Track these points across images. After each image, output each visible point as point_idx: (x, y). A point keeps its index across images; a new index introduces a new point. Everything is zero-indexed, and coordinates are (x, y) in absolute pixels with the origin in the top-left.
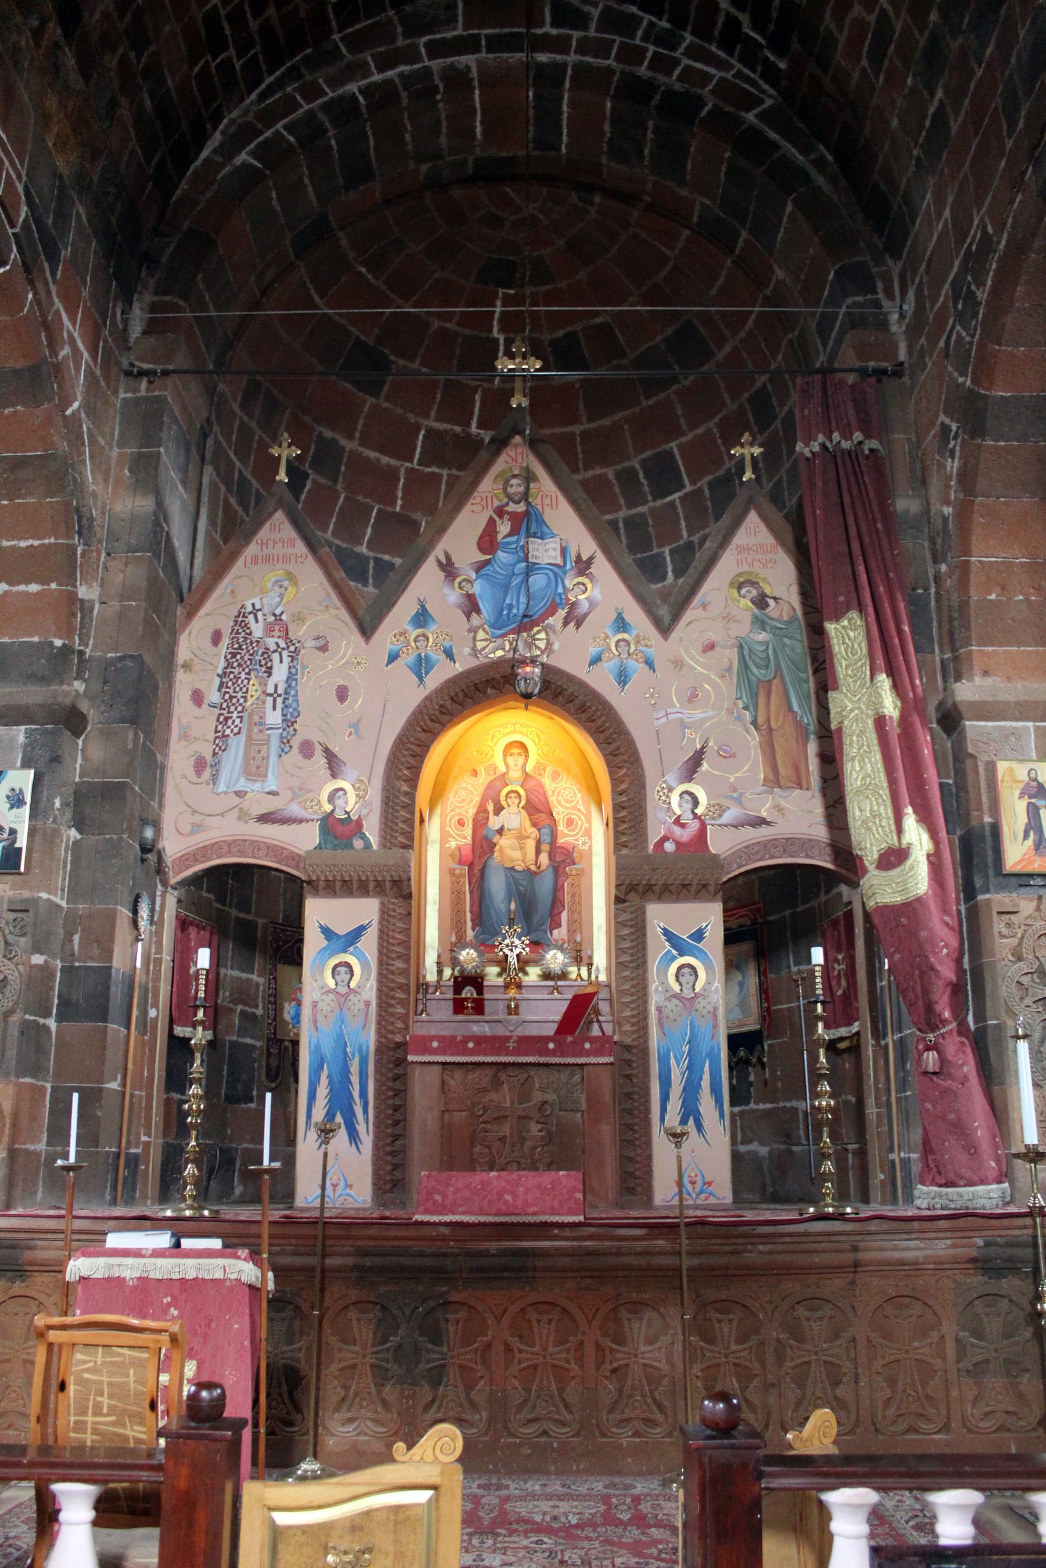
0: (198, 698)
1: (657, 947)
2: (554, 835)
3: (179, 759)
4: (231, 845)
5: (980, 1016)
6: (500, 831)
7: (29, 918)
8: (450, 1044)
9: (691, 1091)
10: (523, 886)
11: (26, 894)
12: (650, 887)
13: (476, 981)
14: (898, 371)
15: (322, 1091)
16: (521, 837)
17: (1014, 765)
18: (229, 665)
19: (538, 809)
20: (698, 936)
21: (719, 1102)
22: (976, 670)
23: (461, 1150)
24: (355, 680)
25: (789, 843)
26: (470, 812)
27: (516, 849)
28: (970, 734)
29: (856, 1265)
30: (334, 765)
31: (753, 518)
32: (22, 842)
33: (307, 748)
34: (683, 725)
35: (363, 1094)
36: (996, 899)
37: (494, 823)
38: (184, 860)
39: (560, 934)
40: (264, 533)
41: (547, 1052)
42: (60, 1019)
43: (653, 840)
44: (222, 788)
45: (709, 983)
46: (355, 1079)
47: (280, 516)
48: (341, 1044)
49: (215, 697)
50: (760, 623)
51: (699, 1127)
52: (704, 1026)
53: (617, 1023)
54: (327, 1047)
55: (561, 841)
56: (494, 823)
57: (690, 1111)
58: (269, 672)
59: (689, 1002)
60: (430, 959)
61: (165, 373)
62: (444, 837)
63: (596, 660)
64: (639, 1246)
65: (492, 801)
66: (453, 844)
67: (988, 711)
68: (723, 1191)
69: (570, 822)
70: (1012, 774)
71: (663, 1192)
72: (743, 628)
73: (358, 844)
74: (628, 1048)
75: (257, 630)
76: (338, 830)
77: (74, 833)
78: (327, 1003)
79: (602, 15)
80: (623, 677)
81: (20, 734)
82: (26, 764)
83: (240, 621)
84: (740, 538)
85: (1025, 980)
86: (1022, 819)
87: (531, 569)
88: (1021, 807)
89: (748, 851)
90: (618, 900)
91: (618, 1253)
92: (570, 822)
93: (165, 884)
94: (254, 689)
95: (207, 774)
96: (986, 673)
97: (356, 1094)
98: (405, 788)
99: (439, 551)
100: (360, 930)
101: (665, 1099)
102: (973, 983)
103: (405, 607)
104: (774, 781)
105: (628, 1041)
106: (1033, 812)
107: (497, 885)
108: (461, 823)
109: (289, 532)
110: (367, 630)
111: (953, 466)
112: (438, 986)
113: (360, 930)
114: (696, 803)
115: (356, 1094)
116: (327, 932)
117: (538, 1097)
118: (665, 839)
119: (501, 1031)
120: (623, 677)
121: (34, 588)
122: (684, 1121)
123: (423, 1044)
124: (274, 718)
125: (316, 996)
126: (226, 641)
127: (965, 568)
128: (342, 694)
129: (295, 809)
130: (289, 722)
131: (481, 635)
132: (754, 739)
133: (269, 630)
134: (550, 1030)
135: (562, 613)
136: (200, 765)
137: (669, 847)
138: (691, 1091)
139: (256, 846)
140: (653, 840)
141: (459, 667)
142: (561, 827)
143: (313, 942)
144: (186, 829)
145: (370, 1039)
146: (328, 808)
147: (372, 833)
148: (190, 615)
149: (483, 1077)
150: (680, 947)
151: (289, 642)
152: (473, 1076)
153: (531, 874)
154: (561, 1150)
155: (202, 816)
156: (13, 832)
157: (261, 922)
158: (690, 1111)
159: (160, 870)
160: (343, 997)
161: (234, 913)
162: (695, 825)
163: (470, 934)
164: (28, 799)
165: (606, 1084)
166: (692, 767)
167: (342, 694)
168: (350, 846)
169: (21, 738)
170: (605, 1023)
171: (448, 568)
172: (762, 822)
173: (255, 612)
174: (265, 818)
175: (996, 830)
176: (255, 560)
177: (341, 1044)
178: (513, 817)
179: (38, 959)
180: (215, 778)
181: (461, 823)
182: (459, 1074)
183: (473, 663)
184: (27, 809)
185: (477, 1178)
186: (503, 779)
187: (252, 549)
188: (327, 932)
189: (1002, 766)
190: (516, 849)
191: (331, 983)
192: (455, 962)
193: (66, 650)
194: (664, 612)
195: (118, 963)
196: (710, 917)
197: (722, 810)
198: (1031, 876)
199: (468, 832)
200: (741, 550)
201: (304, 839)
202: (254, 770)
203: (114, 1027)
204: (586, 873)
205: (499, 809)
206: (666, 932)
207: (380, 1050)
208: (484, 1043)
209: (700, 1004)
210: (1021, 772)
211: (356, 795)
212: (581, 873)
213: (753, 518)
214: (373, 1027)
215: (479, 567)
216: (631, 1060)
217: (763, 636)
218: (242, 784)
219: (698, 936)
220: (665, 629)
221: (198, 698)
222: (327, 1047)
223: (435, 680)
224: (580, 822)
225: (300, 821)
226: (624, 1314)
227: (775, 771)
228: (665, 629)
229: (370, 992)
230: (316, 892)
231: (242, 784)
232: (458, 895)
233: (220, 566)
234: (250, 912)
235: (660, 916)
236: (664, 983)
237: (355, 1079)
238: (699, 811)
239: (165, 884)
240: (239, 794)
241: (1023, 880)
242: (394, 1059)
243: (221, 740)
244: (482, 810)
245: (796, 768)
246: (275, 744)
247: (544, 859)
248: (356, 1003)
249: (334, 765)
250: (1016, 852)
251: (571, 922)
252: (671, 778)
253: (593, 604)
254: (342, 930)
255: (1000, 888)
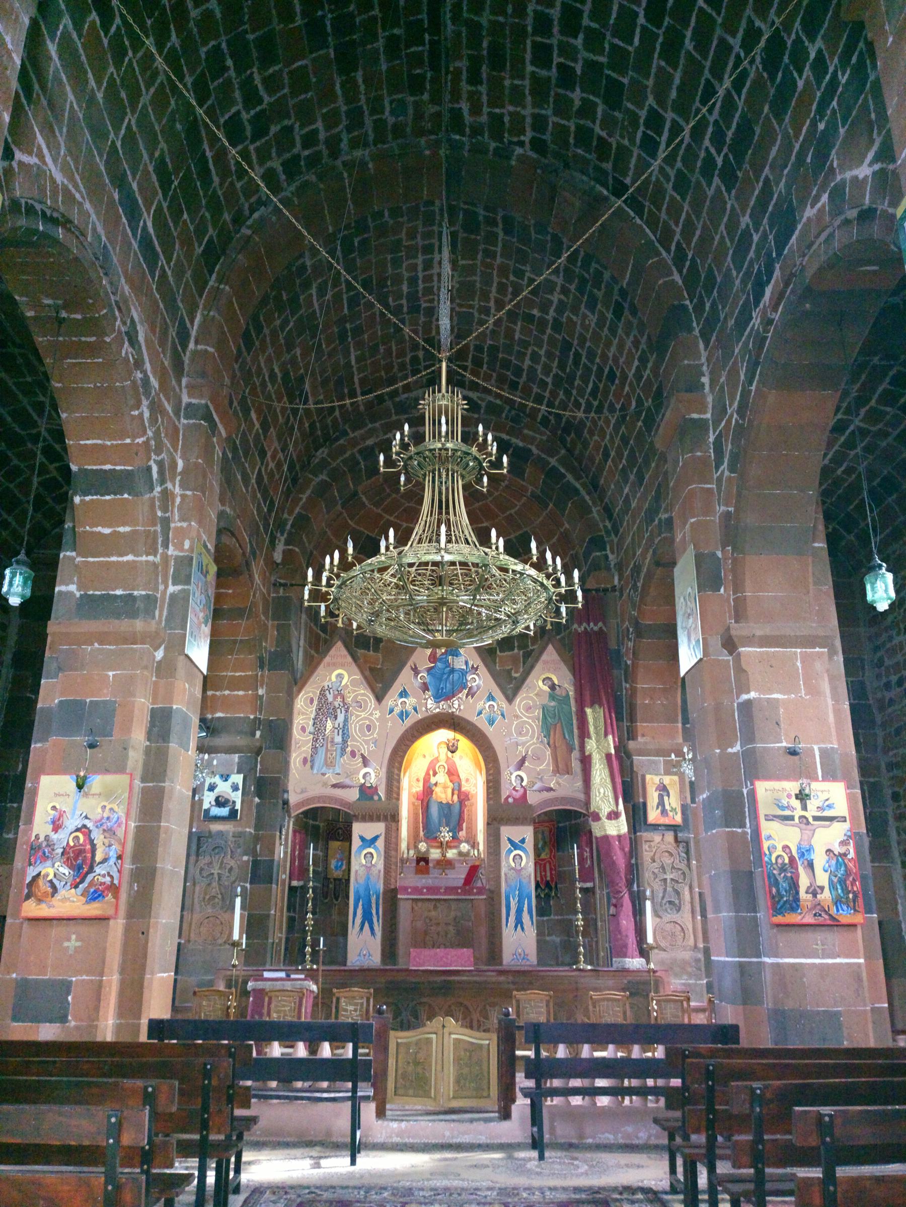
0: (303, 729)
1: (505, 846)
2: (460, 786)
3: (295, 759)
4: (319, 798)
5: (638, 886)
6: (436, 784)
7: (241, 841)
8: (416, 890)
9: (519, 911)
10: (446, 808)
11: (240, 829)
12: (502, 819)
13: (426, 860)
14: (614, 589)
15: (360, 911)
16: (445, 787)
17: (654, 777)
18: (318, 714)
19: (452, 773)
20: (523, 841)
21: (531, 918)
22: (639, 733)
23: (422, 940)
24: (372, 720)
25: (563, 800)
26: (422, 775)
27: (443, 793)
28: (635, 762)
29: (577, 989)
30: (365, 762)
31: (550, 647)
32: (238, 806)
33: (353, 754)
34: (517, 744)
35: (377, 913)
36: (645, 835)
37: (433, 780)
38: (299, 805)
39: (462, 834)
40: (332, 652)
41: (458, 894)
42: (251, 883)
43: (503, 797)
44: (315, 771)
45: (527, 863)
46: (374, 906)
47: (339, 644)
48: (367, 889)
49: (310, 728)
50: (552, 697)
51: (523, 929)
52: (525, 881)
53: (488, 881)
54: (362, 892)
55: (463, 789)
56: (433, 780)
57: (519, 922)
58: (336, 717)
59: (519, 871)
60: (404, 845)
61: (292, 585)
62: (410, 787)
63: (480, 713)
64: (494, 979)
65: (432, 770)
66: (414, 790)
67: (641, 753)
68: (533, 959)
69: (467, 780)
70: (652, 780)
71: (508, 958)
72: (545, 700)
73: (376, 798)
74: (492, 892)
75: (330, 698)
76: (367, 792)
77: (257, 800)
78: (362, 871)
79: (487, 407)
80: (491, 722)
81: (236, 757)
82: (239, 772)
83: (322, 694)
84: (544, 657)
85: (656, 871)
86: (656, 800)
87: (453, 671)
88: (656, 795)
89: (546, 802)
90: (488, 824)
91: (485, 982)
92: (467, 780)
93: (289, 816)
94: (329, 725)
95: (309, 764)
96: (643, 735)
97: (374, 912)
98: (396, 771)
99: (410, 663)
100: (376, 838)
101: (508, 915)
102: (634, 871)
103: (397, 688)
104: (557, 771)
105: (492, 888)
106: (661, 797)
107: (434, 811)
108: (418, 780)
109: (344, 652)
110: (379, 698)
111: (631, 644)
112: (408, 859)
113: (376, 838)
114: (522, 780)
115: (374, 912)
116: (362, 839)
117: (453, 914)
118: (509, 797)
119: (437, 883)
120: (491, 722)
121: (241, 693)
122: (516, 927)
123: (405, 889)
124: (338, 739)
125: (357, 868)
126: (316, 702)
127: (634, 691)
128: (369, 728)
129: (347, 782)
130: (345, 741)
131: (429, 701)
132: (548, 753)
133: (335, 697)
134: (460, 883)
135: (466, 691)
136: (305, 761)
137: (511, 800)
138: (519, 911)
139: (331, 799)
140: (503, 797)
141: (420, 716)
142: (463, 783)
143: (356, 842)
144: (299, 791)
145: (381, 887)
146: (362, 781)
147: (382, 793)
148: (299, 691)
149: (431, 906)
150: (515, 846)
151: (345, 704)
152: (427, 904)
153: (449, 806)
154: (463, 939)
155: (304, 784)
156: (234, 802)
157: (322, 825)
158: (519, 922)
159: (288, 812)
160: (368, 868)
161: (311, 822)
162: (522, 790)
163: (422, 833)
164: (241, 787)
165: (482, 910)
166: (520, 765)
167: (369, 730)
168: (372, 798)
169: (237, 760)
170: (482, 880)
171: (416, 671)
172: (550, 789)
173: (329, 689)
174: (334, 786)
175: (645, 804)
176: (329, 665)
177: (367, 889)
178: (441, 778)
179: (245, 858)
180: (312, 767)
181: (418, 780)
182: (420, 904)
183: (426, 715)
184: (240, 792)
185: (432, 952)
186: (437, 760)
187: (327, 659)
188: (362, 839)
189: (648, 777)
190: (443, 793)
191: (364, 862)
192: (416, 847)
193: (255, 718)
194: (509, 692)
195: (276, 858)
196: (527, 833)
197: (534, 784)
198: (659, 825)
199: (421, 784)
200: (546, 662)
201: (353, 795)
202: (329, 764)
203: (274, 886)
204: (474, 805)
205: (435, 774)
206: (509, 839)
207: (385, 893)
208: (432, 890)
209: (523, 872)
210: (657, 779)
211: (374, 775)
212: (472, 805)
213: (550, 647)
214: (382, 882)
215: (429, 670)
216: (493, 897)
217: (553, 704)
218: (324, 770)
219: (523, 841)
220: (510, 699)
221: (303, 729)
222: (362, 892)
223: (409, 722)
224: (472, 780)
225: (350, 787)
226: (488, 1007)
227: (557, 766)
228: (510, 699)
229: (381, 866)
230: (357, 820)
231: (324, 770)
232: (416, 815)
233: (312, 664)
234: (328, 827)
235: (506, 832)
236: (508, 862)
237: (374, 906)
238: (524, 784)
239: (289, 816)
240: (324, 774)
241: (655, 827)
242: (391, 897)
243: (315, 748)
244: (427, 774)
245: (567, 765)
246: (339, 751)
247: (455, 797)
248: (374, 871)
249: (365, 762)
250: (653, 815)
251: (467, 828)
252: (511, 768)
253: (478, 687)
254: (369, 837)
255: (647, 830)
